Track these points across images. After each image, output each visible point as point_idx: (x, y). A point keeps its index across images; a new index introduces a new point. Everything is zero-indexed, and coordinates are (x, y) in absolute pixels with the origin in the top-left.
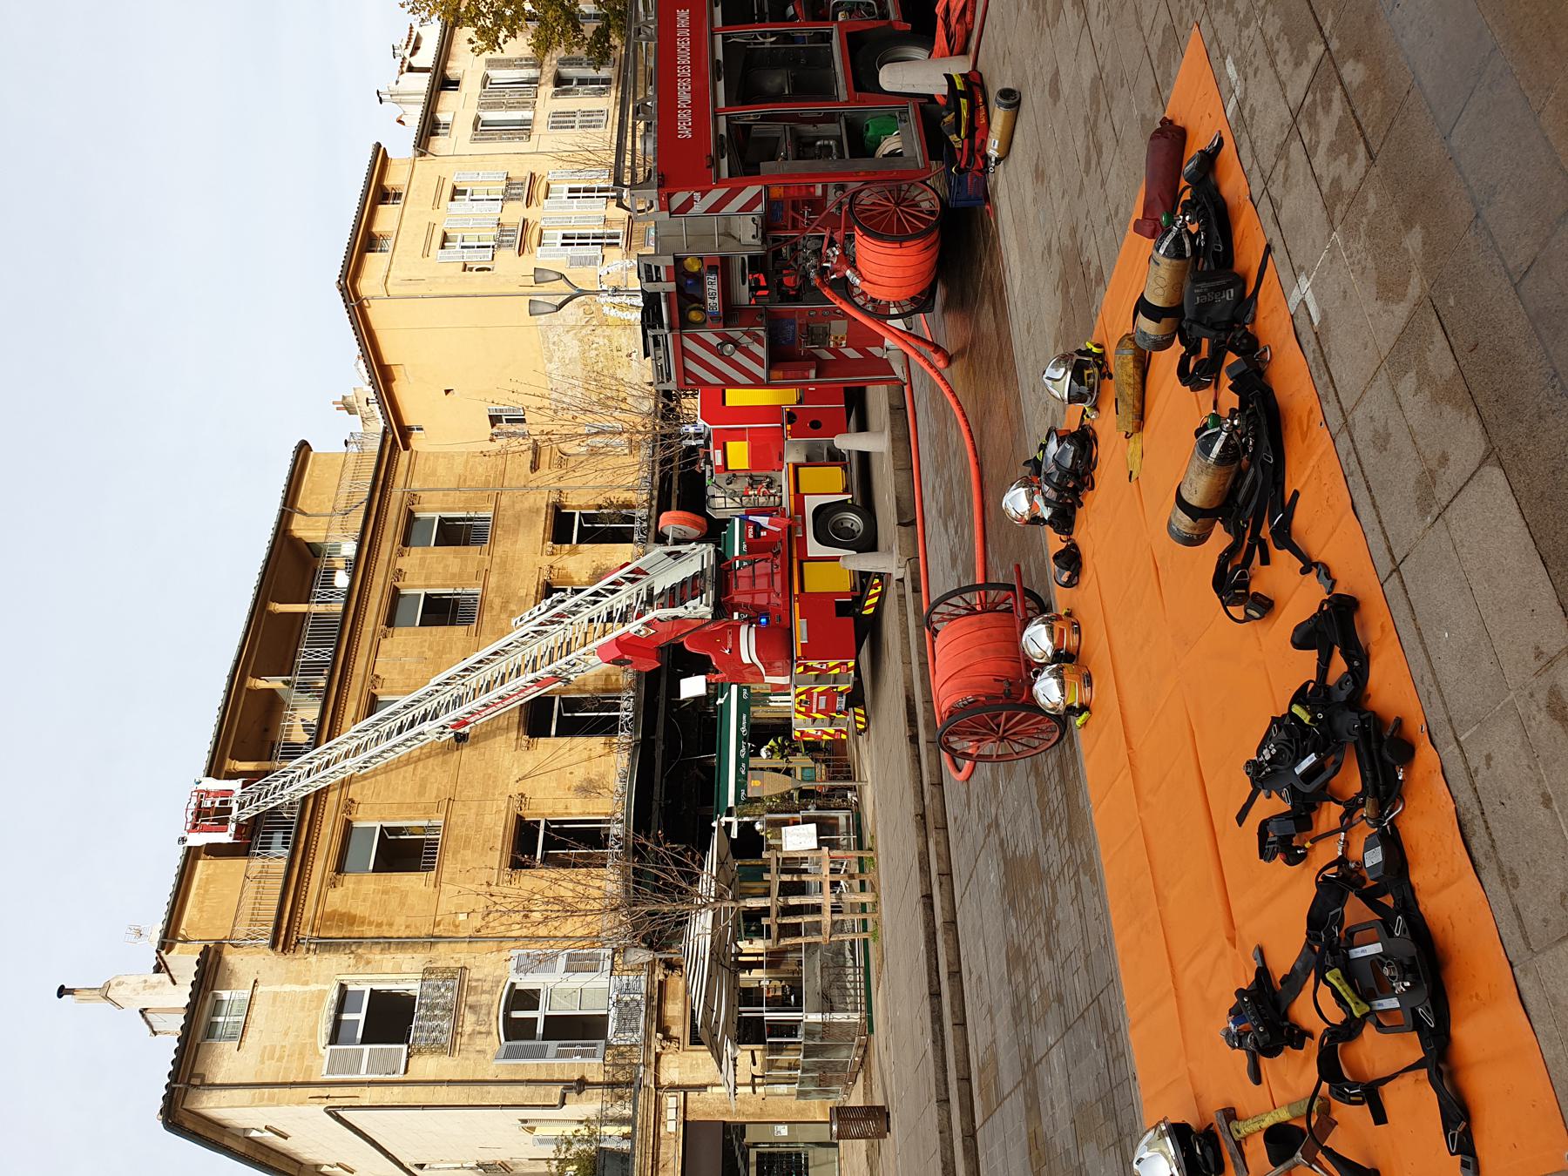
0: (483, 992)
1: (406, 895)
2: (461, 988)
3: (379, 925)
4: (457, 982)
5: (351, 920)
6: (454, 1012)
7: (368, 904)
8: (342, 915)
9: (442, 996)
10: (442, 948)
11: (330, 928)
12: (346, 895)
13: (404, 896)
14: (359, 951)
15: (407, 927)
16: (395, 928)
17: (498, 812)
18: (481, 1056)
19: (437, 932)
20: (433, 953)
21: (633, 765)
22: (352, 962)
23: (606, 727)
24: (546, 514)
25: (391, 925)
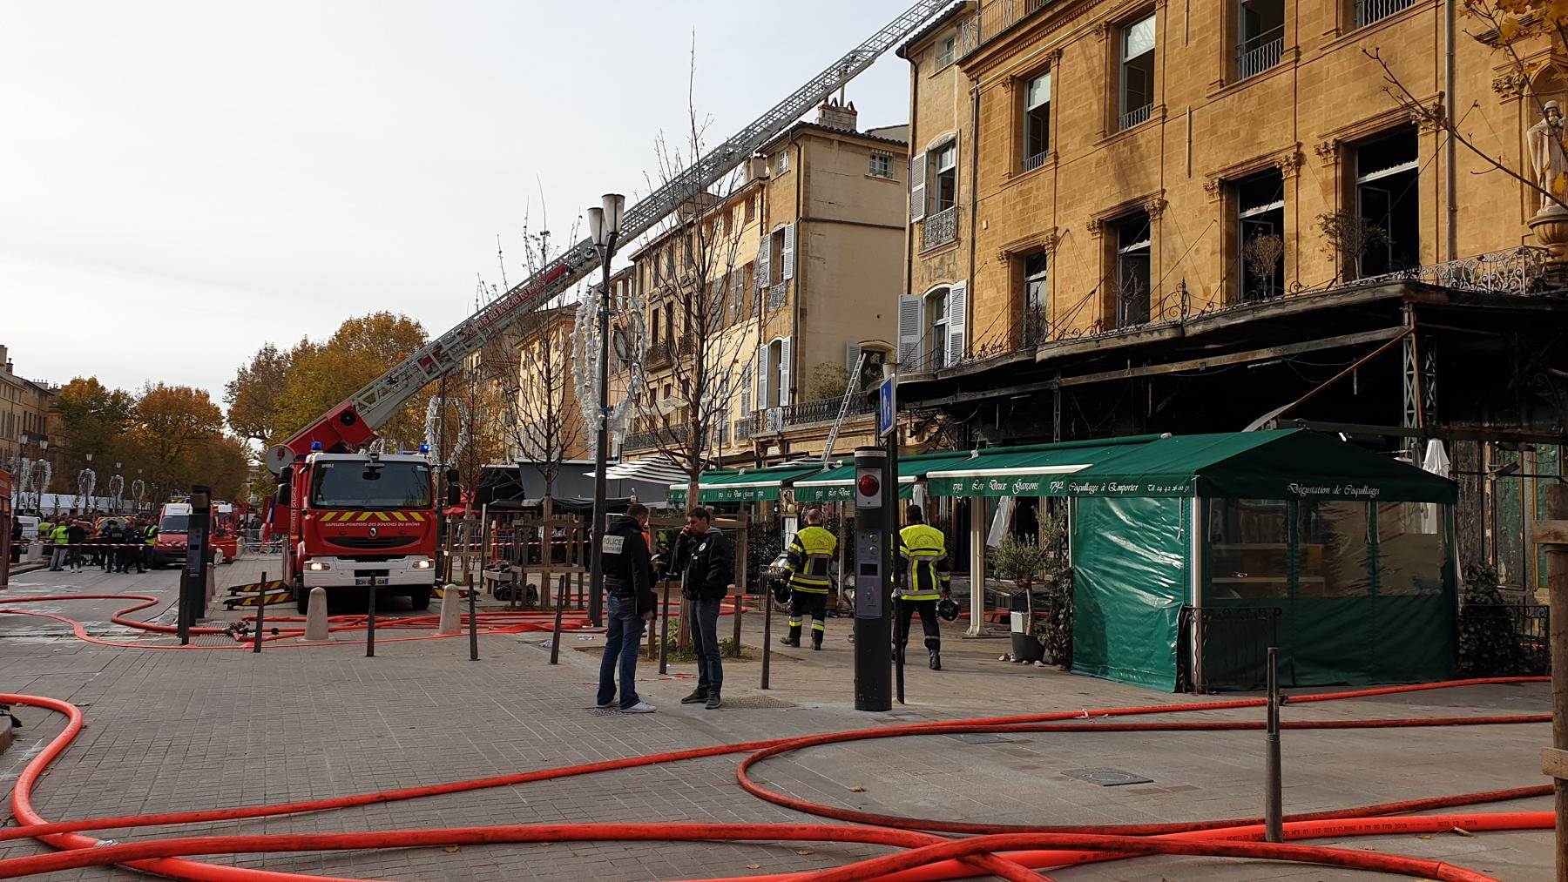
1: (999, 161)
5: (987, 120)
18: (920, 280)
24: (1391, 112)
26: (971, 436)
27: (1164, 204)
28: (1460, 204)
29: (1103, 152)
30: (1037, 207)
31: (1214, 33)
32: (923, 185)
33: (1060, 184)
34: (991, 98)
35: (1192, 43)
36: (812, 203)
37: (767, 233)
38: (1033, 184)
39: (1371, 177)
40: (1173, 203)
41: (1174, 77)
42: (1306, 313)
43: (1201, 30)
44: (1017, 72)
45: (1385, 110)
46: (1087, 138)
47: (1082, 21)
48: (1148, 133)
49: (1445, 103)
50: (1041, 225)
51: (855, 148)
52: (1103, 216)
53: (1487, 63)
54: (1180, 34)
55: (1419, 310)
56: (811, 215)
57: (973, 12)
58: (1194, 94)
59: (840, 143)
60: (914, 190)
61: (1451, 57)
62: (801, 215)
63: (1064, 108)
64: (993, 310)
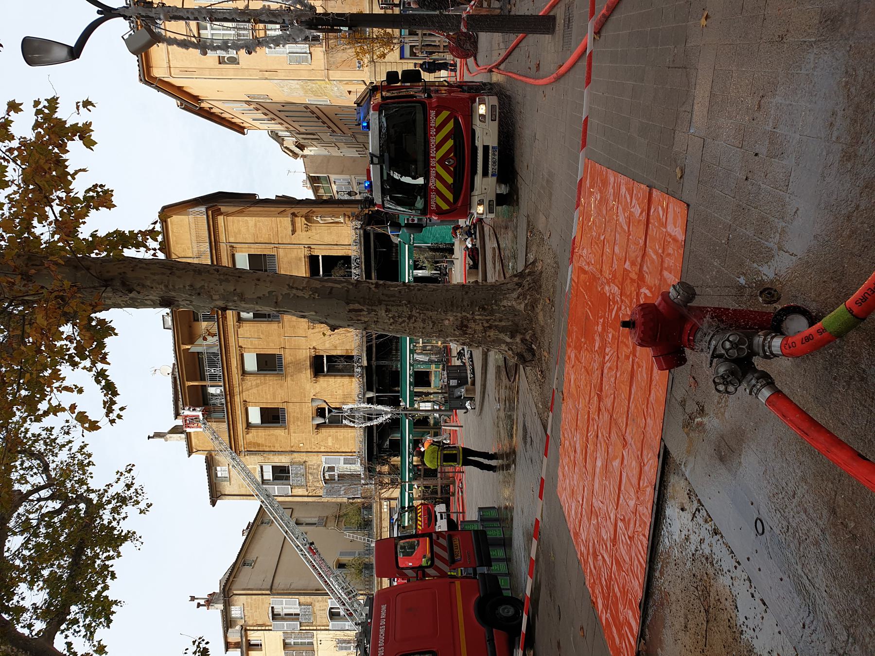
0: (314, 469)
2: (306, 469)
3: (270, 447)
4: (304, 467)
5: (259, 445)
6: (305, 476)
7: (264, 439)
8: (254, 443)
9: (300, 470)
10: (295, 455)
11: (251, 447)
12: (253, 437)
13: (277, 437)
14: (265, 455)
15: (281, 447)
16: (276, 448)
17: (309, 407)
19: (292, 450)
20: (293, 457)
21: (365, 437)
22: (263, 459)
23: (347, 372)
25: (274, 447)
26: (387, 448)
27: (314, 348)
28: (335, 243)
29: (289, 379)
30: (301, 412)
31: (261, 326)
32: (276, 487)
33: (295, 400)
34: (250, 443)
35: (261, 336)
36: (263, 587)
37: (271, 626)
38: (292, 415)
39: (321, 273)
40: (314, 344)
41: (271, 344)
42: (365, 255)
43: (258, 333)
44: (245, 425)
45: (304, 264)
46: (281, 386)
47: (236, 390)
48: (287, 358)
49: (306, 246)
50: (309, 409)
51: (238, 572)
52: (312, 376)
53: (299, 235)
54: (256, 342)
55: (368, 224)
56: (269, 587)
57: (211, 455)
58: (279, 336)
59: (234, 578)
60: (277, 494)
61: (294, 244)
62: (268, 592)
63: (267, 399)
64: (337, 439)
